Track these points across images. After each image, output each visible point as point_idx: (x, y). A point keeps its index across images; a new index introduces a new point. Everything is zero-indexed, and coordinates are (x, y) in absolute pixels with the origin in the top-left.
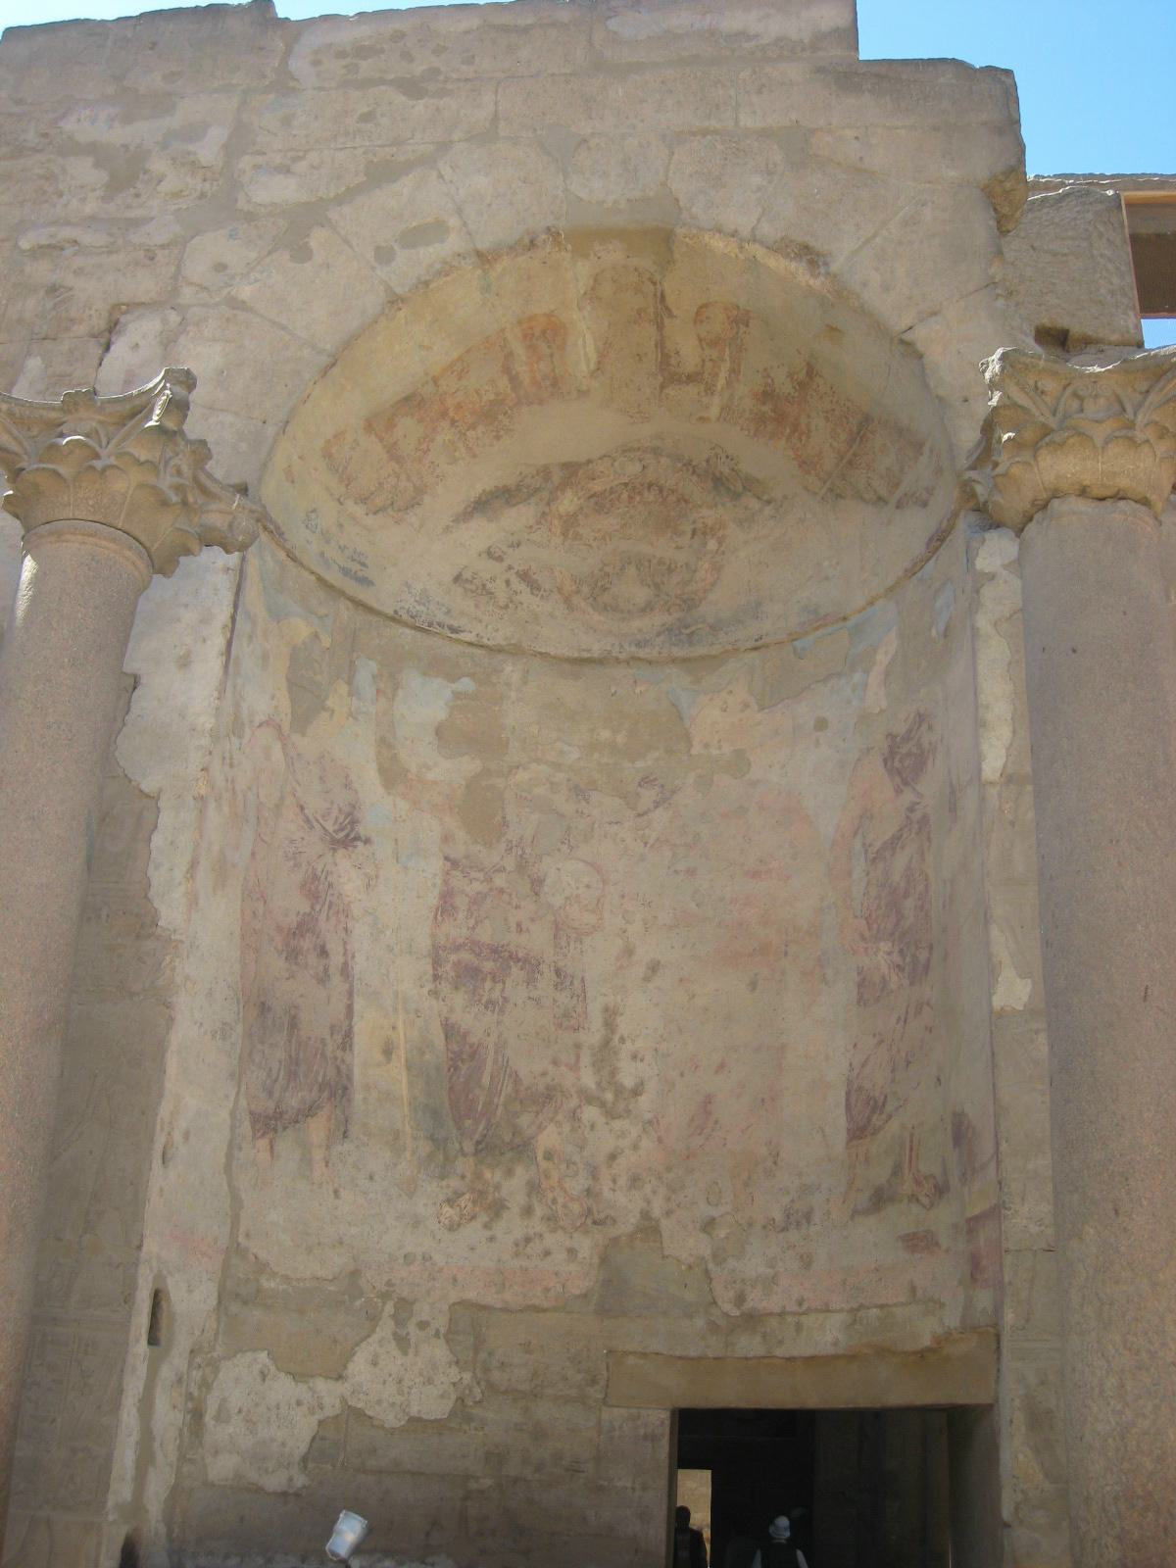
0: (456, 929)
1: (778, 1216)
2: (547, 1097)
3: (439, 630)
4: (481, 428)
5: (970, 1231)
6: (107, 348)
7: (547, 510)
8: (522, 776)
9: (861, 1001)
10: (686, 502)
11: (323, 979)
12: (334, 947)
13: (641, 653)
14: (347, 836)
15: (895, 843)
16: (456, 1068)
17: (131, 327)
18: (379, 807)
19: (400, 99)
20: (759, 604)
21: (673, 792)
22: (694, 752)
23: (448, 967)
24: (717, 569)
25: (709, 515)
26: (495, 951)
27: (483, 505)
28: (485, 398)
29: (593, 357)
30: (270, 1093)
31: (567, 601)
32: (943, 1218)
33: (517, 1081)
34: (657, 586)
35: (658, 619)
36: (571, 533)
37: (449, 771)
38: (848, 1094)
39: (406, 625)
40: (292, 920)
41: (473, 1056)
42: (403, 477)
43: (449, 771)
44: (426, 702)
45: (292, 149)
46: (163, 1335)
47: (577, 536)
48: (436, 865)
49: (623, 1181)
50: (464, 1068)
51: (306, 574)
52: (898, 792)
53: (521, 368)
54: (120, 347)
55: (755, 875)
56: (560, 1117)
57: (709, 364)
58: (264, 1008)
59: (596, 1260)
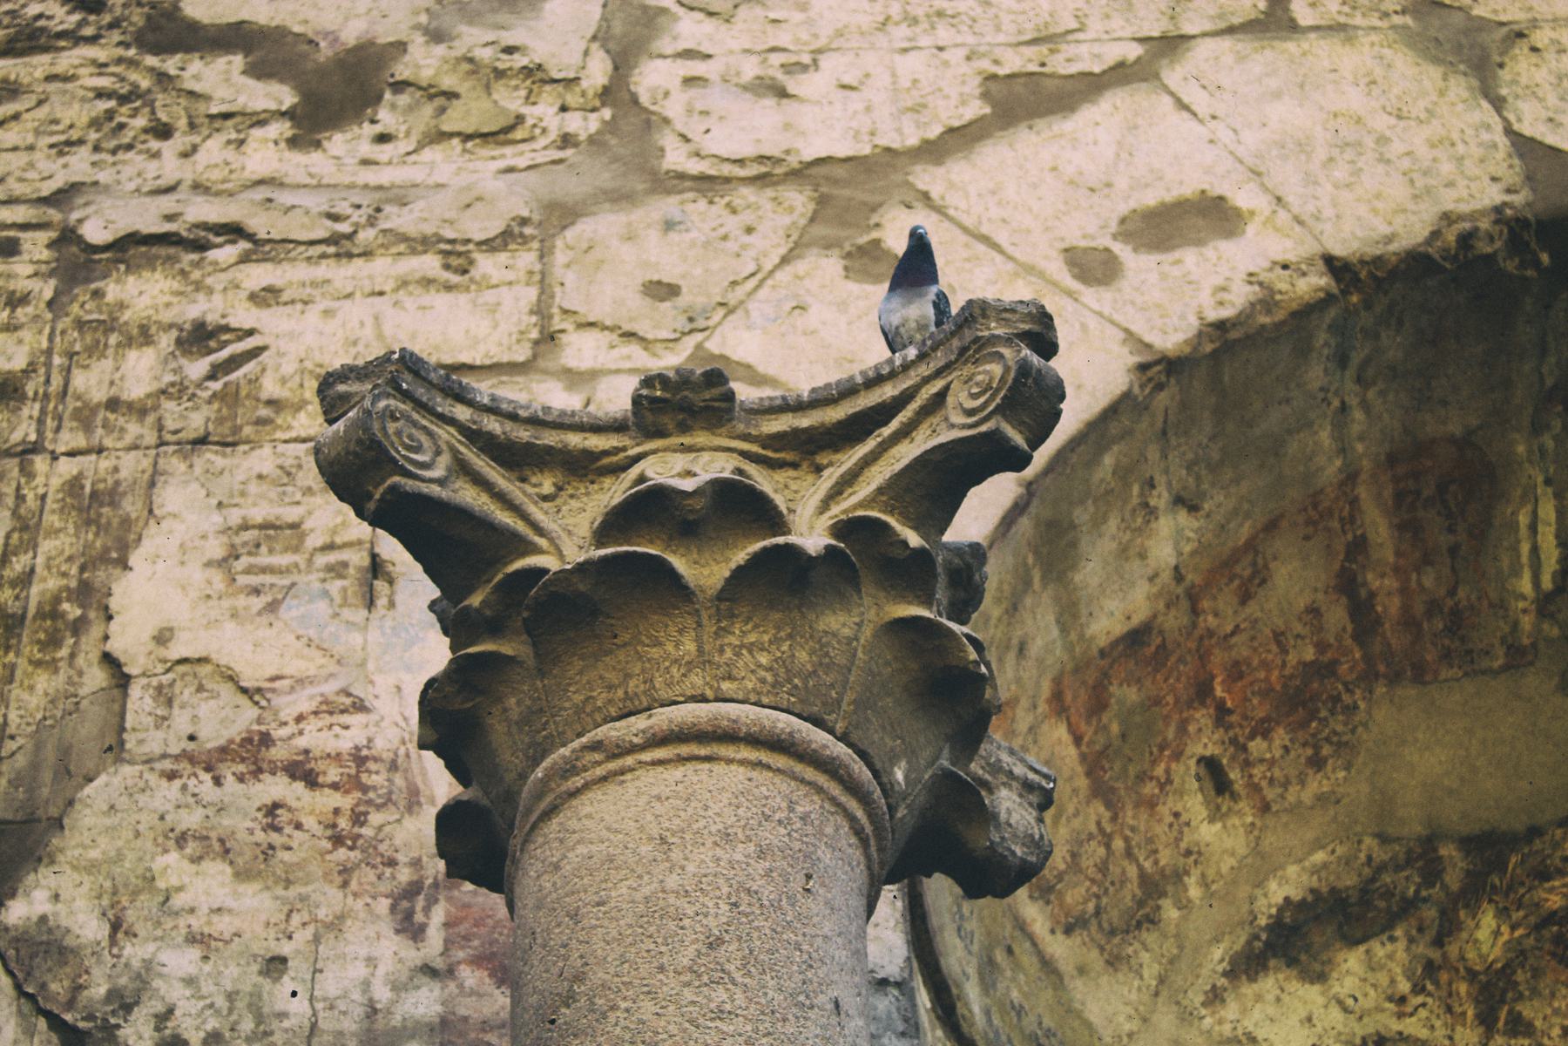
4: (1281, 736)
7: (1436, 955)
28: (1292, 658)
36: (1503, 1015)
42: (1118, 844)
45: (773, 50)
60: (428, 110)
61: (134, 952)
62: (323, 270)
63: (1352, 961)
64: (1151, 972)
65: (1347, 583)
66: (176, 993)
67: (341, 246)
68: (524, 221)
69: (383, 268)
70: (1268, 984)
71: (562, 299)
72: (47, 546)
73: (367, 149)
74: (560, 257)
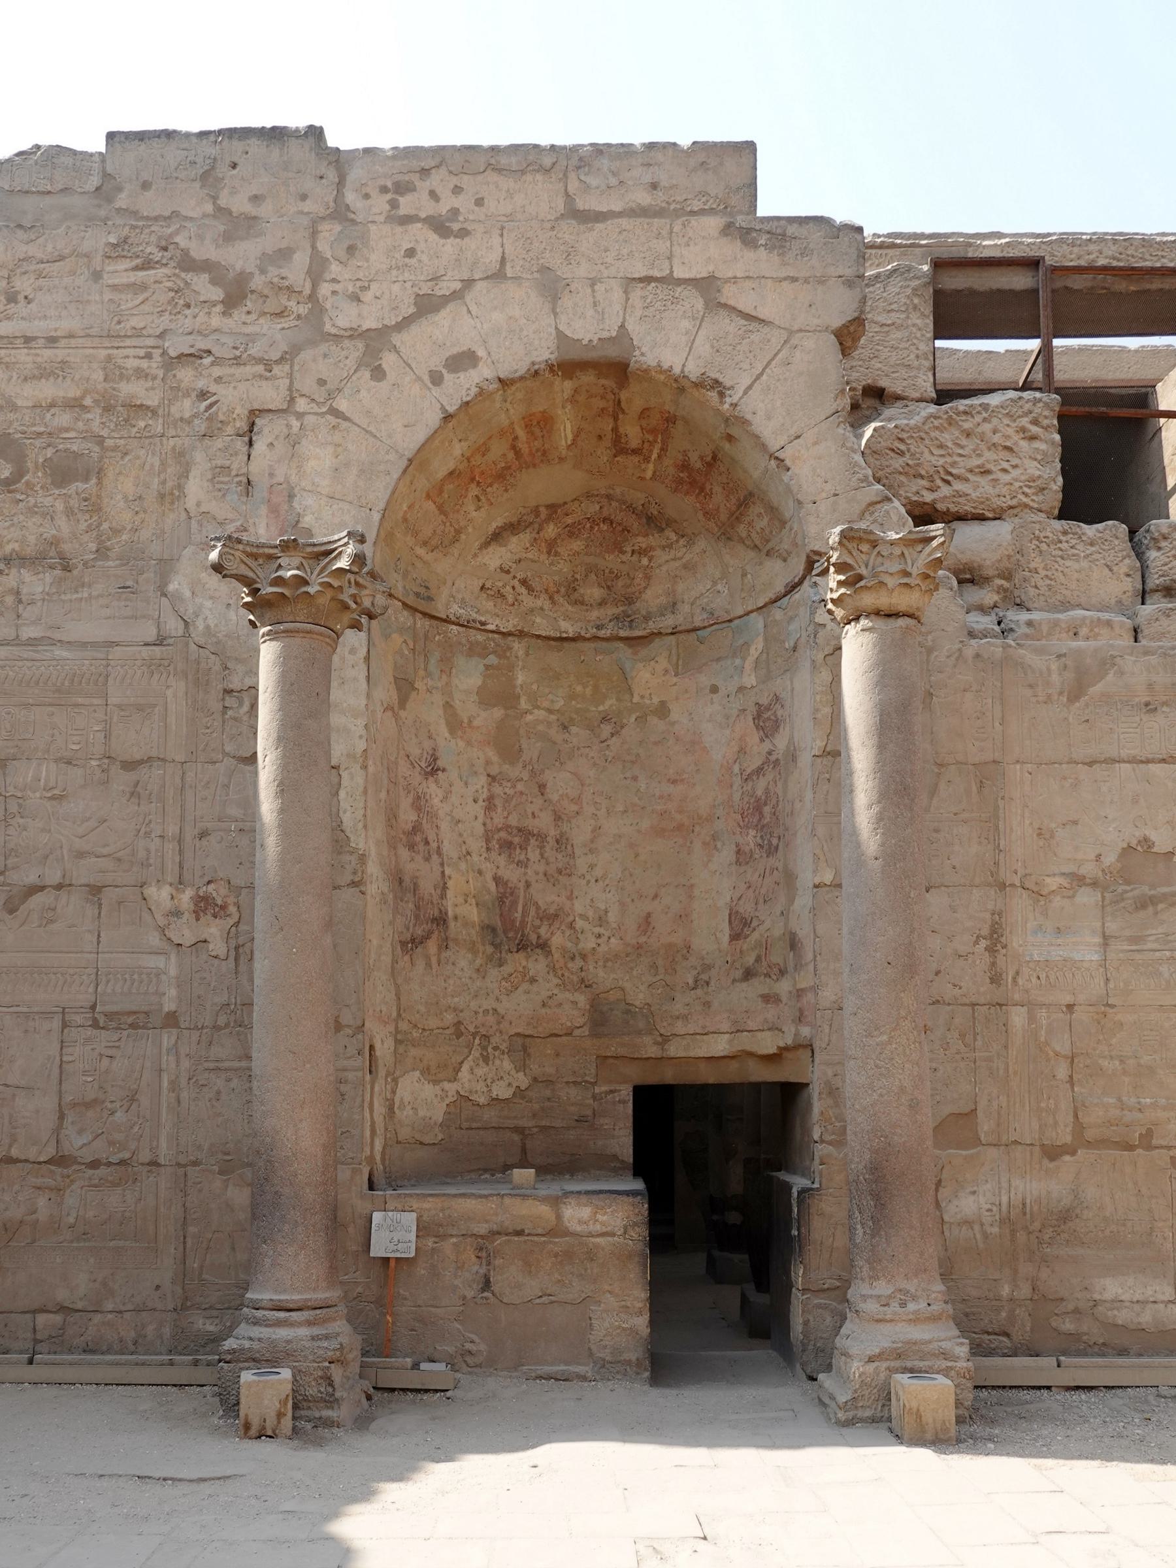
0: (498, 819)
1: (691, 981)
2: (553, 918)
3: (474, 625)
4: (496, 486)
5: (799, 996)
6: (251, 443)
8: (529, 718)
9: (738, 862)
10: (629, 531)
11: (427, 859)
12: (431, 837)
13: (602, 633)
14: (433, 770)
15: (759, 771)
16: (504, 902)
17: (266, 431)
18: (449, 748)
19: (433, 237)
20: (675, 604)
21: (622, 727)
22: (635, 700)
23: (494, 842)
24: (648, 578)
25: (642, 542)
26: (520, 830)
27: (496, 537)
29: (570, 437)
30: (408, 929)
31: (551, 598)
32: (784, 987)
33: (538, 908)
34: (608, 587)
35: (611, 611)
37: (487, 718)
38: (730, 915)
39: (454, 623)
40: (409, 827)
41: (512, 894)
43: (487, 718)
44: (469, 677)
46: (373, 1069)
47: (557, 554)
48: (483, 780)
49: (601, 963)
50: (507, 902)
51: (396, 602)
52: (762, 740)
53: (524, 448)
54: (260, 446)
55: (674, 782)
56: (563, 927)
57: (646, 445)
58: (401, 881)
59: (588, 1007)
60: (261, 301)
61: (198, 600)
62: (232, 370)
63: (514, 539)
64: (456, 555)
65: (513, 447)
66: (208, 613)
67: (237, 361)
68: (286, 353)
69: (249, 370)
70: (490, 549)
71: (296, 385)
72: (169, 470)
73: (244, 317)
74: (296, 368)
